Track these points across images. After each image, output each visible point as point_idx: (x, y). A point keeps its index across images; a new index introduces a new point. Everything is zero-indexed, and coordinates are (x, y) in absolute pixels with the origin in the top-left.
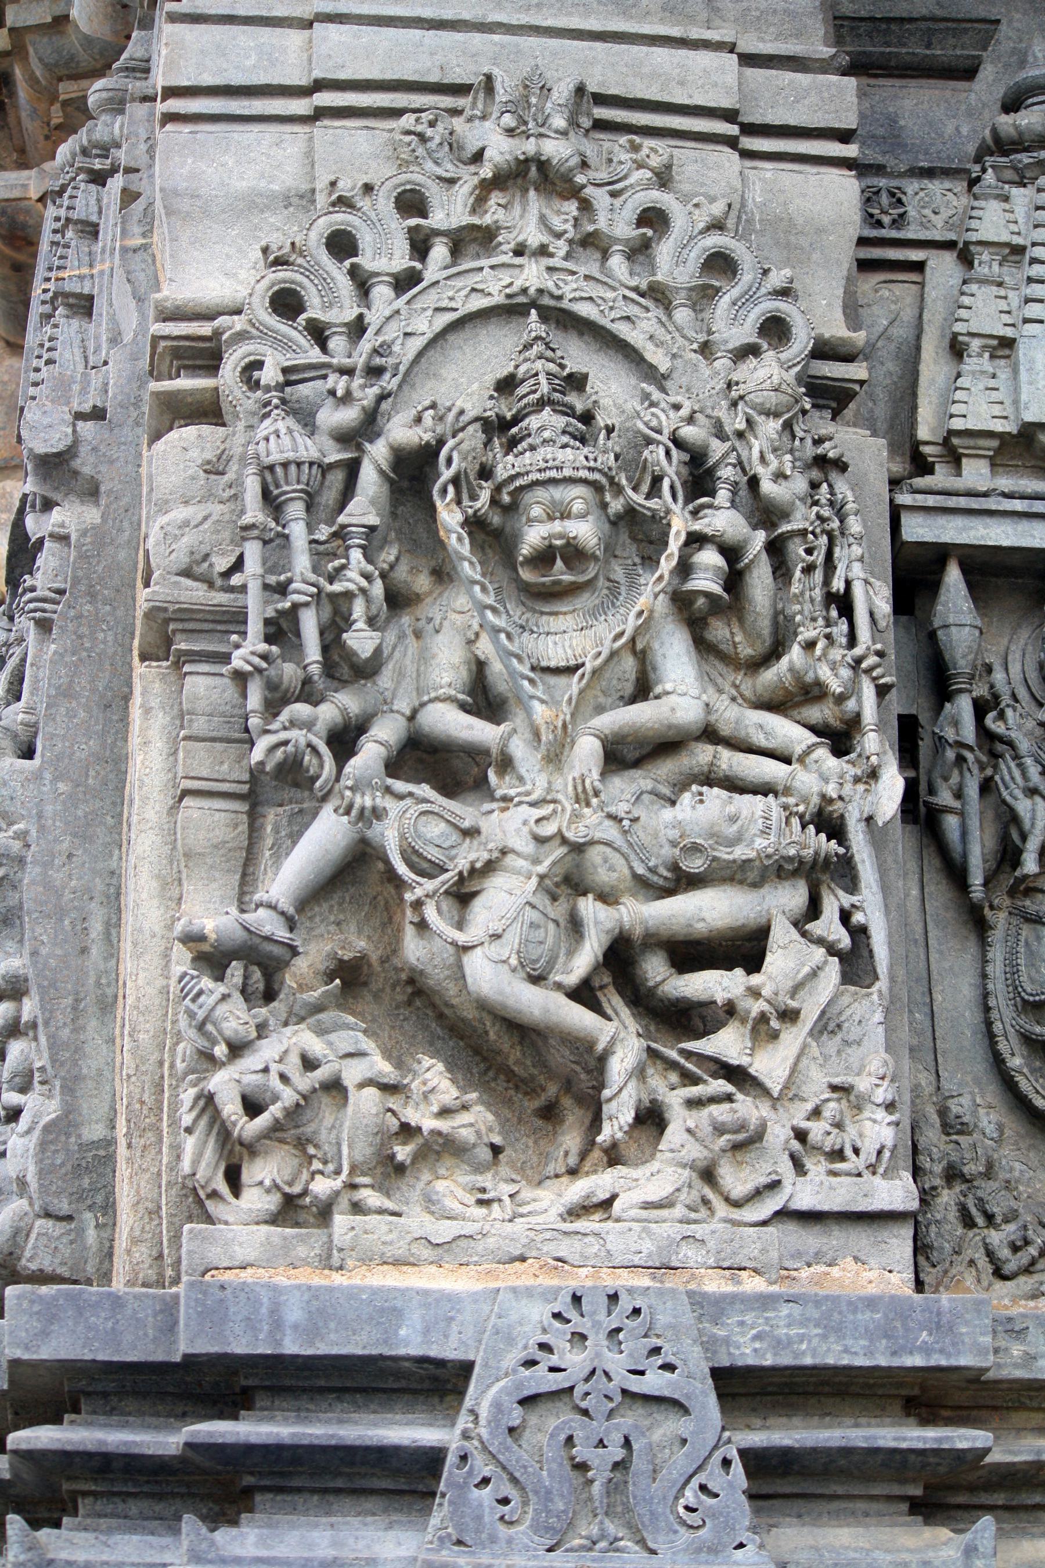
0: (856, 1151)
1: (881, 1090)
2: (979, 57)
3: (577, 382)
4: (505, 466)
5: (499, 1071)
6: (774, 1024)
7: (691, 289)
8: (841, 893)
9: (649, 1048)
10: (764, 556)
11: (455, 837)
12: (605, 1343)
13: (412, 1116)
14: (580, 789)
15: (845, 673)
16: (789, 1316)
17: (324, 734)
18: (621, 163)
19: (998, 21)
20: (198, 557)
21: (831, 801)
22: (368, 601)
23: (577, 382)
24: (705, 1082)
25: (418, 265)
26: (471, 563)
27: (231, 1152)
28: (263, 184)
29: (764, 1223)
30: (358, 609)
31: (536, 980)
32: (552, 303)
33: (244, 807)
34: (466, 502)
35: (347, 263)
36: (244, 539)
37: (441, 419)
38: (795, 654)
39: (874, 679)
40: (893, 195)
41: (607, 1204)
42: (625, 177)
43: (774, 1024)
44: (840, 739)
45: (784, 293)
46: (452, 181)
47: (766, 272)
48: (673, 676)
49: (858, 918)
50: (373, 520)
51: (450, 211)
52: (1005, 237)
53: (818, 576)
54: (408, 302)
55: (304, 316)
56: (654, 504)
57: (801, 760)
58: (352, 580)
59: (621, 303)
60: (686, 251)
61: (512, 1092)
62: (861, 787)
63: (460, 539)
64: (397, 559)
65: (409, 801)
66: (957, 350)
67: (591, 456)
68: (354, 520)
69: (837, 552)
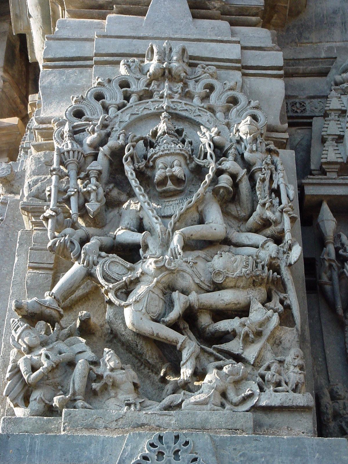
0: (287, 383)
1: (296, 360)
2: (330, 68)
3: (179, 132)
4: (151, 151)
5: (145, 366)
6: (251, 336)
7: (222, 107)
8: (279, 293)
9: (201, 348)
10: (246, 177)
11: (125, 271)
12: (173, 456)
13: (99, 370)
14: (174, 253)
15: (278, 214)
16: (256, 446)
17: (78, 239)
18: (198, 71)
19: (336, 58)
20: (40, 191)
21: (274, 258)
22: (97, 194)
23: (179, 132)
24: (224, 360)
25: (126, 102)
26: (135, 181)
27: (28, 391)
28: (75, 84)
29: (247, 411)
30: (93, 196)
31: (156, 321)
32: (173, 111)
33: (52, 272)
34: (136, 163)
35: (101, 101)
36: (52, 175)
37: (128, 138)
38: (258, 207)
39: (289, 214)
40: (301, 104)
41: (179, 406)
42: (200, 76)
43: (251, 336)
44: (278, 240)
45: (256, 108)
46: (139, 79)
47: (250, 102)
48: (212, 217)
49: (287, 302)
50: (99, 168)
51: (137, 87)
52: (339, 107)
53: (267, 182)
54: (122, 112)
55: (85, 117)
56: (205, 161)
57: (262, 246)
58: (91, 187)
59: (197, 111)
60: (221, 96)
61: (150, 374)
62: (286, 255)
63: (132, 174)
64: (113, 188)
65: (107, 258)
66: (323, 141)
67: (181, 146)
68: (93, 168)
69: (274, 176)
